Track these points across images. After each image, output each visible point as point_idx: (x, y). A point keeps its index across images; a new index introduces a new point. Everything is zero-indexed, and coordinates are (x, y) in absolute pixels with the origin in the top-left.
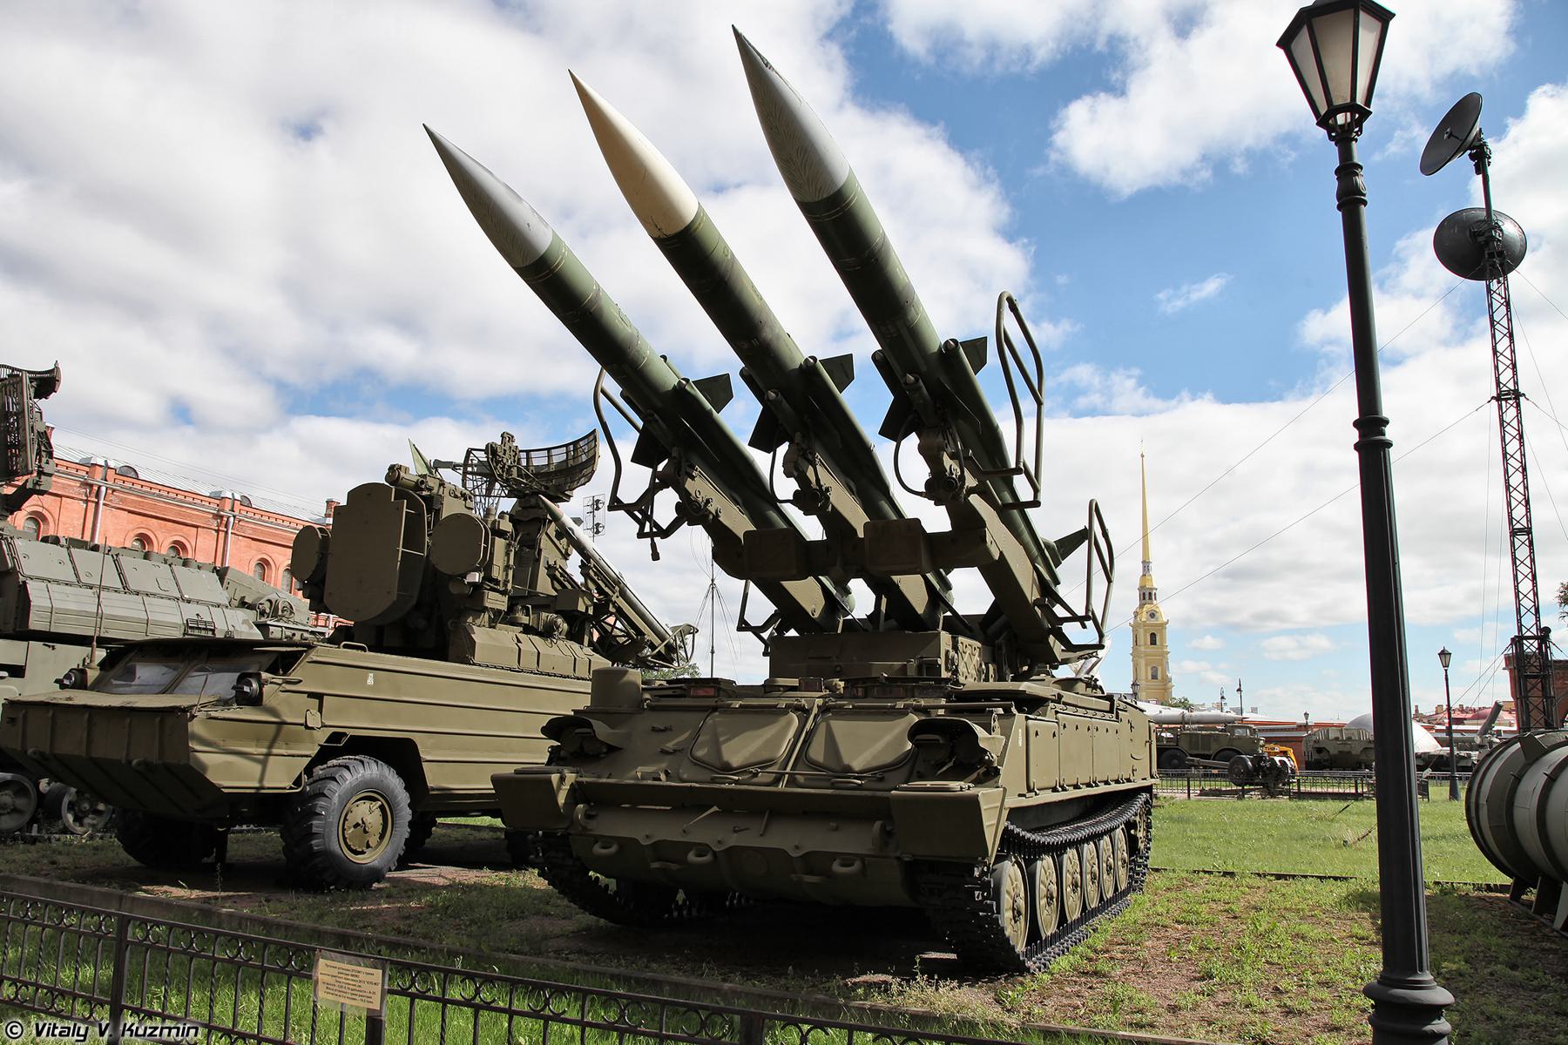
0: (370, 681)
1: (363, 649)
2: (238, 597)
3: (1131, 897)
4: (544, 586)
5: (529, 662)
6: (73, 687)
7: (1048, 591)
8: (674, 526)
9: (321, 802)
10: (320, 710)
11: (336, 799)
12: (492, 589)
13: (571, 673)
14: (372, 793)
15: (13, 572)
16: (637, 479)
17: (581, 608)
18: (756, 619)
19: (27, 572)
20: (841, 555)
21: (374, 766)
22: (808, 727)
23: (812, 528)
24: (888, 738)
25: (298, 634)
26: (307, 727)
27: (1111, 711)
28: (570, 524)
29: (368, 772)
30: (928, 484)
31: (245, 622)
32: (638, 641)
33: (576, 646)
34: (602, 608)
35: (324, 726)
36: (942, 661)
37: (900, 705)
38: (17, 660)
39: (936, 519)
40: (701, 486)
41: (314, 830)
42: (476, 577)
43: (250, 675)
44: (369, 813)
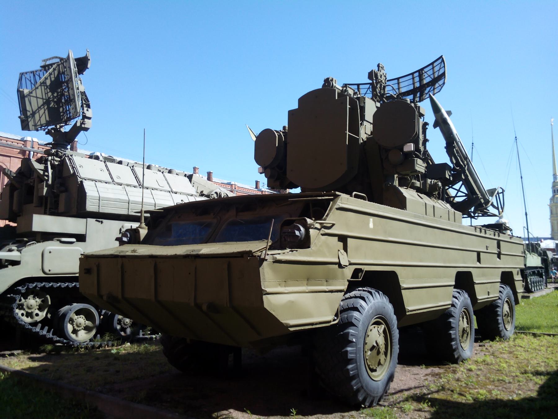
0: (371, 225)
2: (199, 192)
6: (129, 242)
9: (351, 331)
10: (345, 249)
11: (360, 325)
14: (381, 319)
15: (75, 176)
17: (447, 177)
28: (446, 115)
29: (376, 301)
35: (351, 264)
41: (350, 356)
43: (293, 221)
44: (376, 335)
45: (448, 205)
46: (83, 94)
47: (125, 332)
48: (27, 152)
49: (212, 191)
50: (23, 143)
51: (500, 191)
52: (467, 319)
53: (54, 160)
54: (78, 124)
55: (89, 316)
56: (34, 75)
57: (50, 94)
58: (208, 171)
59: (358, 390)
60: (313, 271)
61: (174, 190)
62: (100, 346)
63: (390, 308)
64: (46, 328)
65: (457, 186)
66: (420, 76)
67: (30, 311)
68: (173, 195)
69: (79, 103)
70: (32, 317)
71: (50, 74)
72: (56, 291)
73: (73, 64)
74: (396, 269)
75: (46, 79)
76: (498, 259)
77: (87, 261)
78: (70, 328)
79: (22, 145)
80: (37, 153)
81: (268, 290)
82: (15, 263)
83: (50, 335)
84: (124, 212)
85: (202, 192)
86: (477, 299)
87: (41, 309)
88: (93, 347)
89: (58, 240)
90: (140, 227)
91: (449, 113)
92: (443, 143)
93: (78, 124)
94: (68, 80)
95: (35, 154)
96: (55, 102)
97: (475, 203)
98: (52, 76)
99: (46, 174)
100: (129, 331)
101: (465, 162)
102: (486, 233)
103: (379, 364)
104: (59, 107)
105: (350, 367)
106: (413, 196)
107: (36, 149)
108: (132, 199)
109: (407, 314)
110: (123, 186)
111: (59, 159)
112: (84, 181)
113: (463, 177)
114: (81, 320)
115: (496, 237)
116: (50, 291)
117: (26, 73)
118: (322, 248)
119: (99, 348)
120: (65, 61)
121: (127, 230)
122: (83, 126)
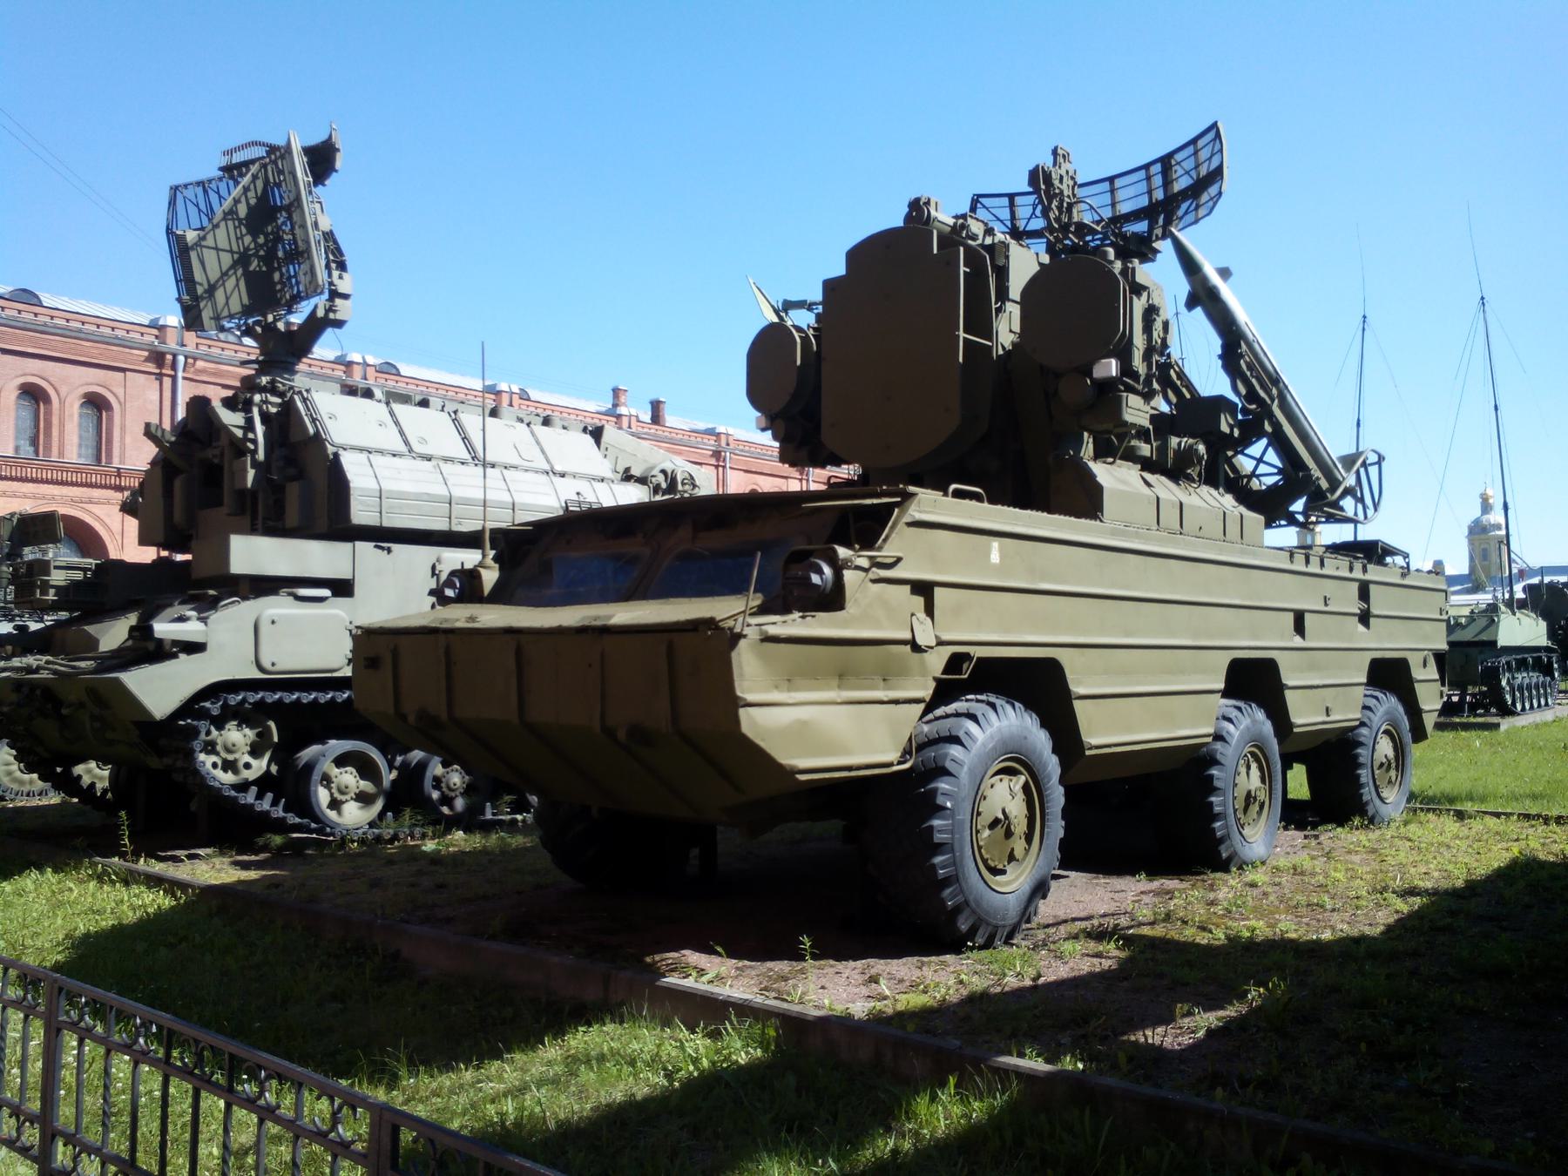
0: (995, 557)
2: (621, 469)
6: (460, 599)
9: (943, 785)
10: (929, 610)
11: (964, 774)
14: (1016, 762)
15: (318, 440)
17: (1225, 428)
21: (1008, 708)
26: (916, 648)
28: (1215, 279)
29: (1005, 723)
35: (941, 643)
38: (340, 571)
41: (938, 837)
42: (1111, 367)
43: (809, 554)
44: (1006, 797)
45: (1228, 500)
46: (329, 236)
47: (451, 807)
48: (169, 357)
49: (652, 468)
50: (155, 332)
51: (1373, 458)
52: (1261, 768)
53: (266, 402)
54: (320, 313)
55: (366, 769)
56: (205, 191)
57: (248, 239)
58: (654, 397)
59: (957, 910)
60: (853, 660)
61: (558, 468)
62: (395, 838)
63: (1041, 741)
64: (269, 796)
65: (1256, 449)
67: (233, 758)
68: (557, 480)
69: (319, 261)
70: (236, 772)
71: (246, 190)
72: (292, 713)
73: (300, 164)
74: (1061, 655)
75: (237, 201)
76: (1361, 628)
77: (373, 644)
78: (323, 796)
79: (152, 339)
80: (195, 359)
81: (750, 697)
82: (194, 648)
83: (279, 812)
84: (439, 525)
85: (627, 470)
86: (1291, 725)
87: (255, 751)
88: (378, 839)
89: (290, 594)
90: (481, 565)
91: (1225, 273)
92: (1213, 343)
94: (291, 204)
95: (190, 361)
96: (260, 258)
97: (1305, 488)
98: (251, 194)
99: (251, 436)
101: (1274, 391)
102: (1322, 564)
103: (1012, 858)
104: (271, 271)
105: (938, 860)
106: (1124, 482)
107: (190, 348)
108: (457, 493)
109: (1088, 753)
110: (433, 462)
111: (278, 400)
112: (341, 452)
113: (1268, 428)
114: (348, 778)
115: (1358, 574)
116: (277, 711)
117: (186, 186)
118: (871, 607)
119: (391, 841)
120: (277, 154)
121: (453, 573)
122: (331, 316)
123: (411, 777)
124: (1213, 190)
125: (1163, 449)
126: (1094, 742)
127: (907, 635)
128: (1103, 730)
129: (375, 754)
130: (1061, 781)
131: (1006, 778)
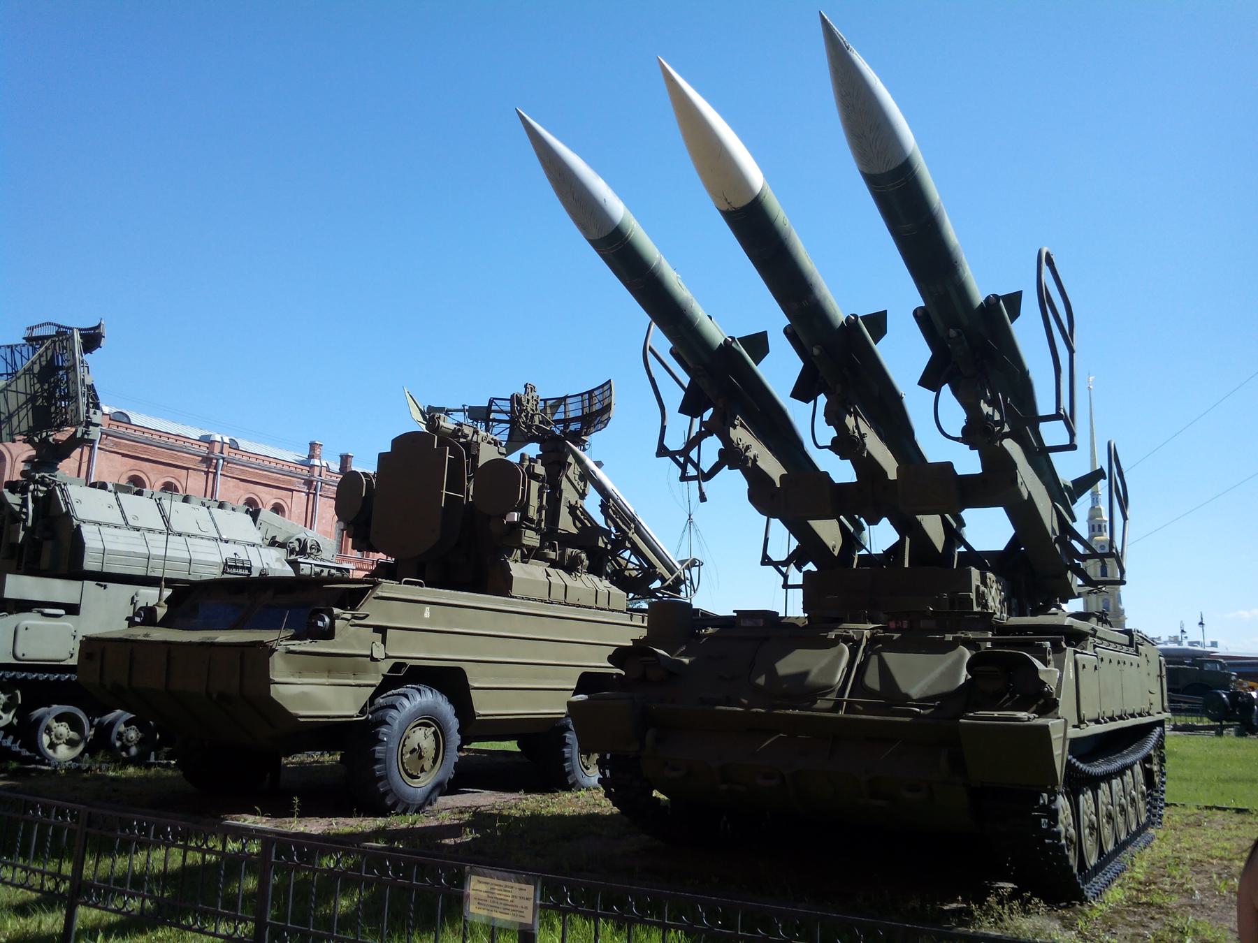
0: (427, 614)
1: (421, 585)
2: (269, 537)
3: (1152, 831)
4: (566, 523)
5: (558, 594)
6: (142, 624)
7: (1066, 530)
8: (716, 469)
11: (396, 726)
12: (528, 528)
13: (593, 604)
14: (428, 719)
15: (68, 516)
16: (680, 429)
17: (601, 544)
18: (778, 554)
19: (80, 516)
20: (870, 496)
21: (429, 693)
22: (858, 661)
23: (842, 472)
24: (941, 668)
25: (326, 571)
26: (373, 659)
27: (1131, 645)
30: (964, 430)
31: (278, 560)
32: (649, 573)
33: (596, 579)
34: (618, 545)
35: (387, 657)
36: (973, 596)
37: (949, 637)
39: (968, 462)
40: (741, 435)
41: (378, 755)
42: (516, 516)
43: (322, 611)
44: (423, 738)
46: (91, 388)
47: (128, 753)
53: (37, 490)
54: (79, 435)
55: (75, 724)
57: (37, 386)
58: (344, 452)
59: (386, 794)
60: (335, 665)
61: (224, 537)
62: (89, 769)
63: (446, 709)
64: (11, 737)
66: (590, 398)
68: (222, 545)
69: (82, 401)
71: (40, 356)
75: (34, 363)
77: (91, 647)
78: (46, 739)
81: (277, 680)
83: (16, 748)
84: (140, 571)
85: (274, 537)
88: (79, 769)
90: (157, 605)
91: (599, 464)
93: (79, 435)
94: (69, 368)
96: (44, 398)
98: (43, 359)
100: (133, 751)
103: (422, 770)
106: (529, 574)
108: (154, 552)
114: (63, 729)
116: (23, 684)
118: (349, 636)
119: (86, 771)
120: (63, 334)
121: (141, 608)
123: (104, 732)
124: (606, 417)
125: (562, 555)
126: (481, 712)
127: (369, 653)
128: (485, 706)
129: (82, 715)
130: (459, 731)
131: (423, 729)
